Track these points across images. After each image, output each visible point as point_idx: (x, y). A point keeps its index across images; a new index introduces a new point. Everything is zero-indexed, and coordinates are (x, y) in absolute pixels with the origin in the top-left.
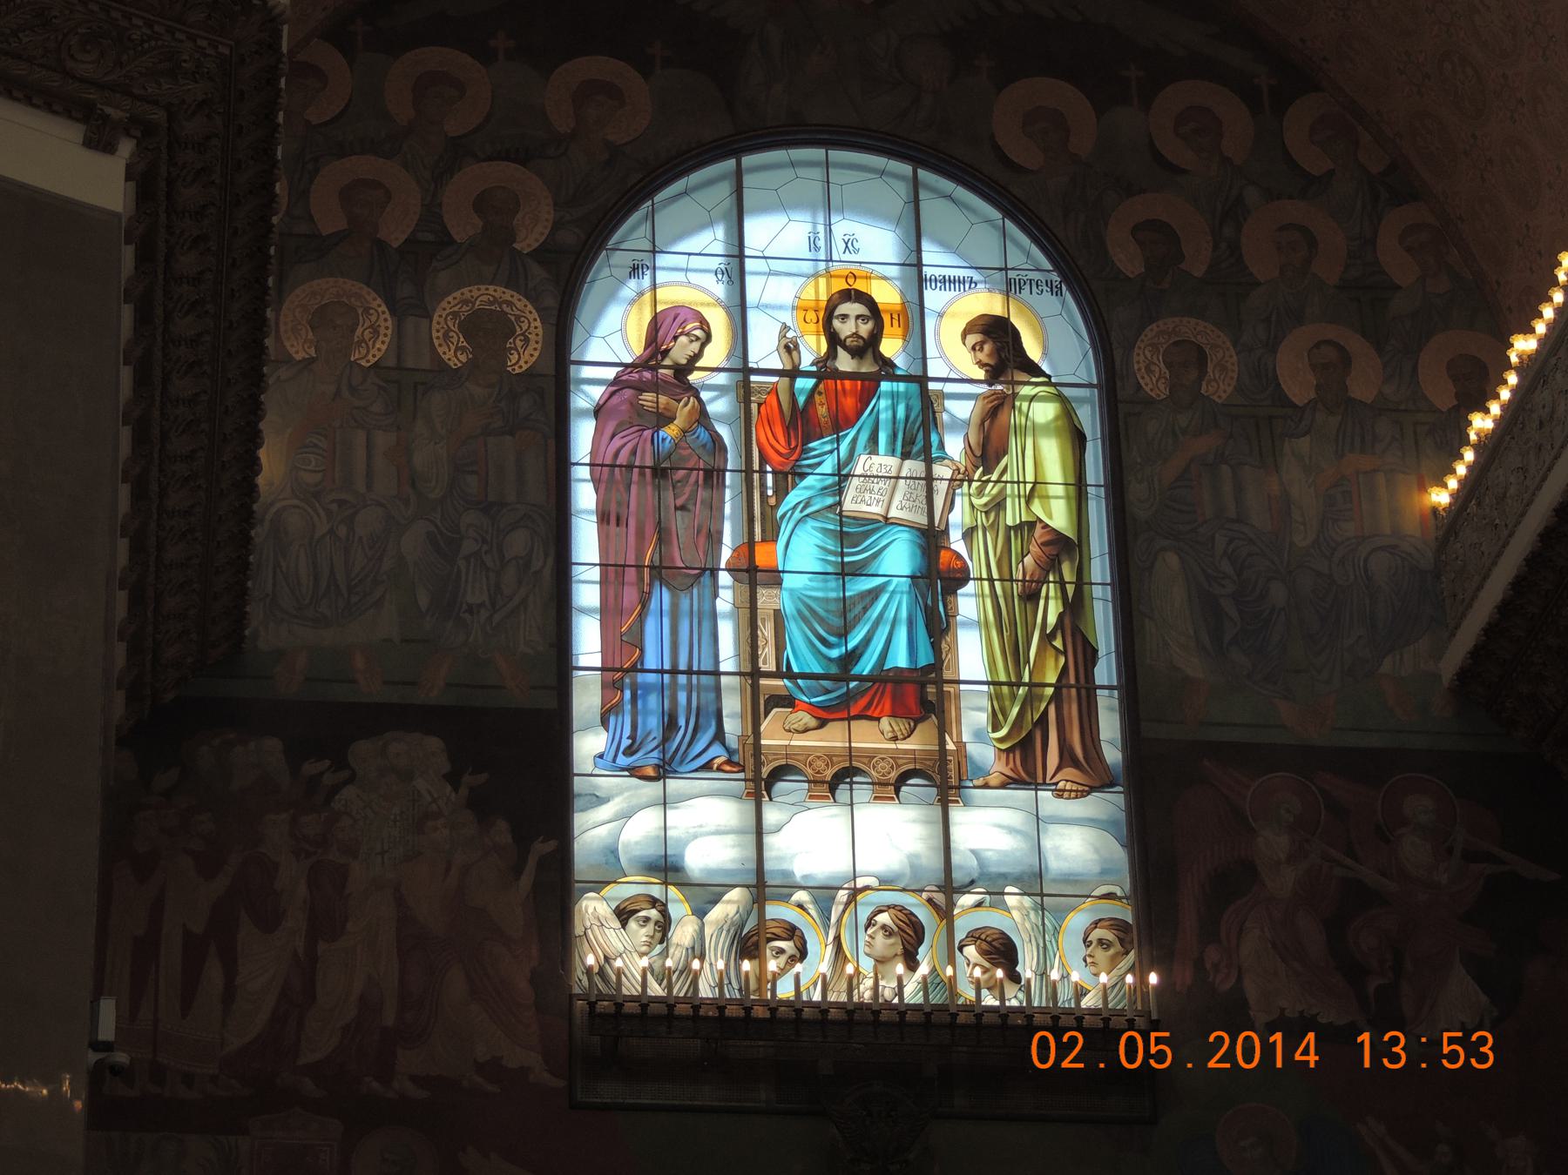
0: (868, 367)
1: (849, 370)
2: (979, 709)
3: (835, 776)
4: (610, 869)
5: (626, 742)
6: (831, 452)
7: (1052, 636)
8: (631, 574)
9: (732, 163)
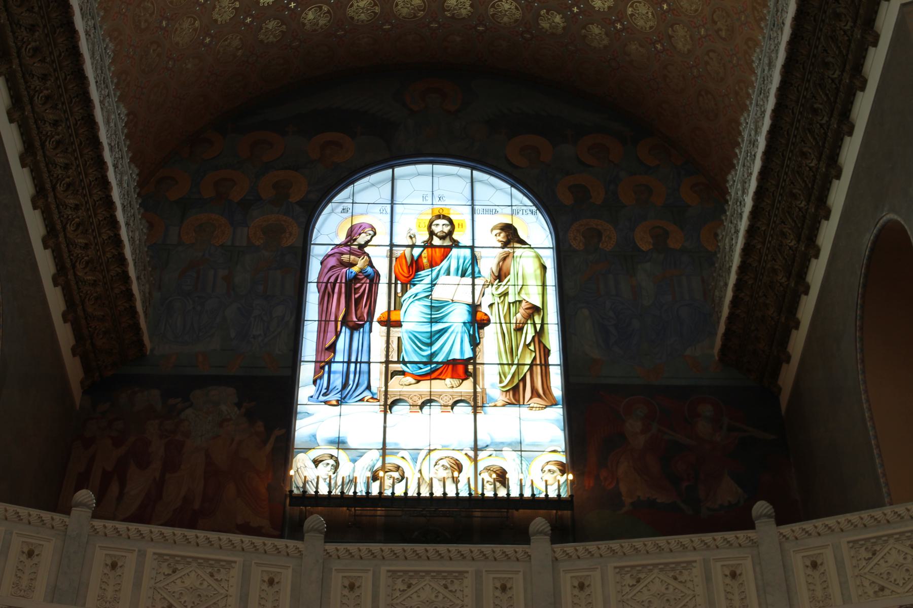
0: (447, 243)
5: (324, 391)
7: (529, 344)
8: (332, 324)
9: (391, 170)
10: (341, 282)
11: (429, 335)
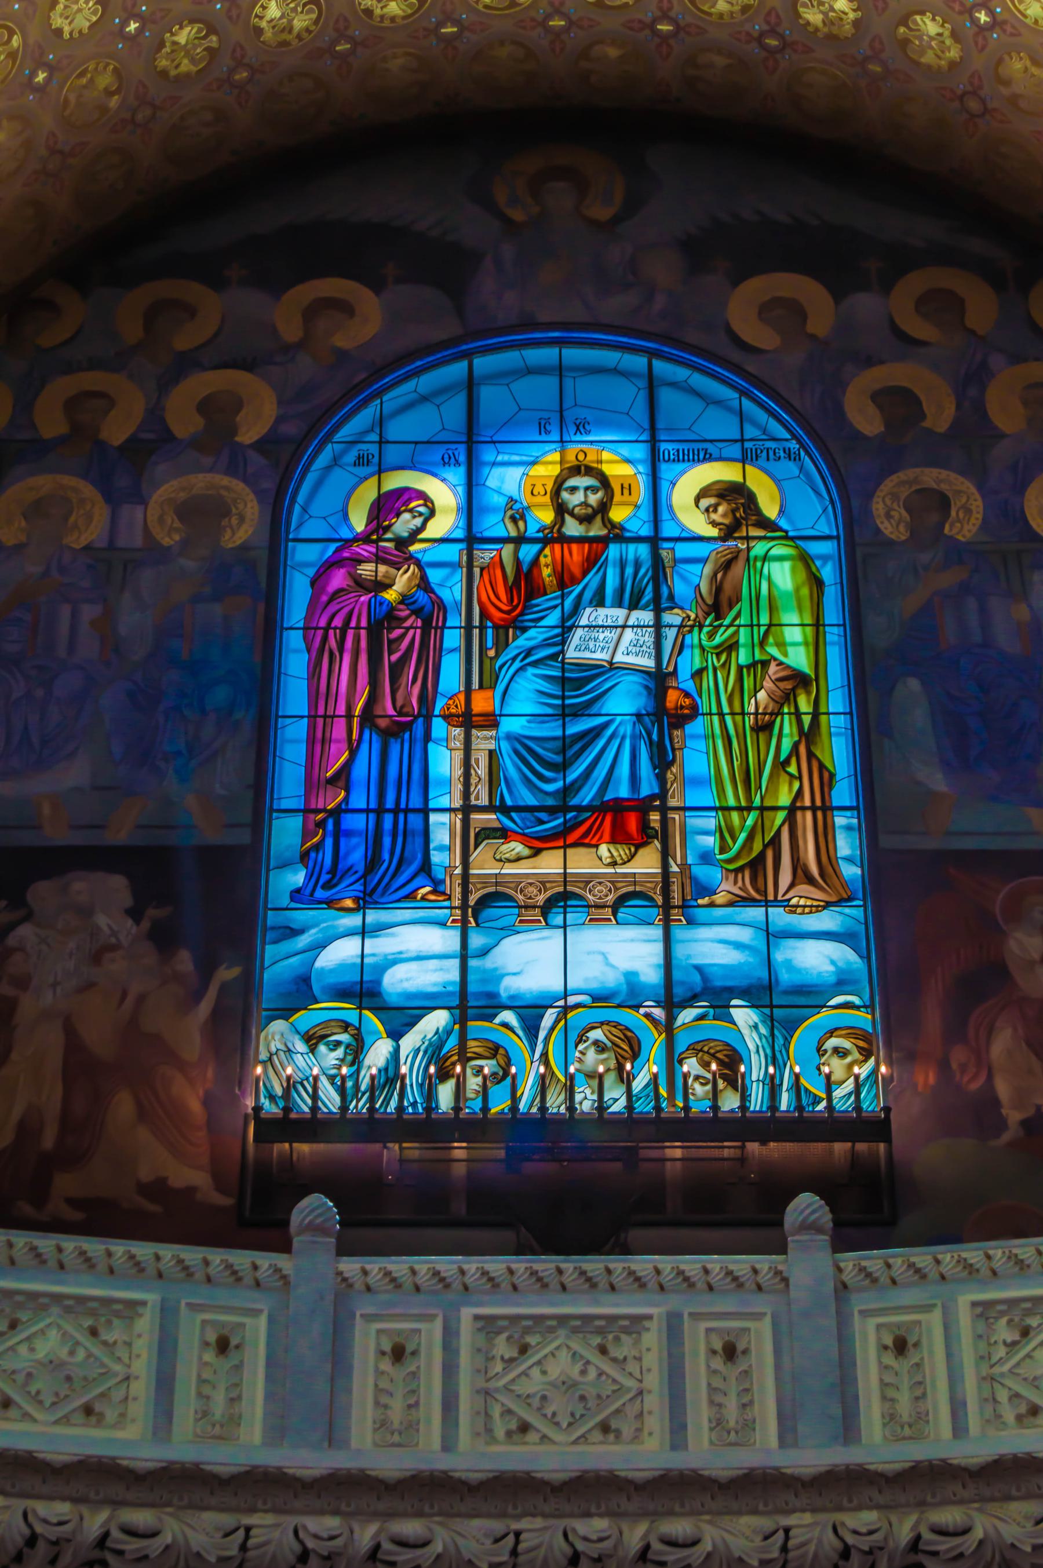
0: (597, 530)
1: (576, 534)
2: (707, 833)
3: (549, 901)
4: (301, 992)
5: (325, 877)
6: (555, 607)
7: (787, 762)
10: (358, 627)
11: (559, 744)
